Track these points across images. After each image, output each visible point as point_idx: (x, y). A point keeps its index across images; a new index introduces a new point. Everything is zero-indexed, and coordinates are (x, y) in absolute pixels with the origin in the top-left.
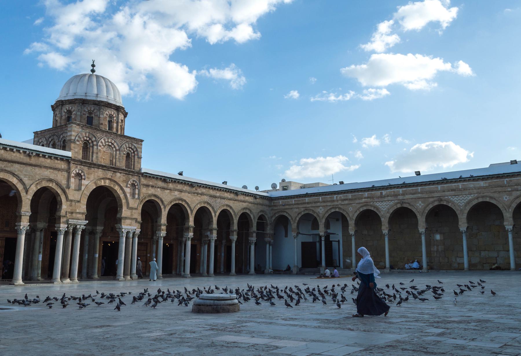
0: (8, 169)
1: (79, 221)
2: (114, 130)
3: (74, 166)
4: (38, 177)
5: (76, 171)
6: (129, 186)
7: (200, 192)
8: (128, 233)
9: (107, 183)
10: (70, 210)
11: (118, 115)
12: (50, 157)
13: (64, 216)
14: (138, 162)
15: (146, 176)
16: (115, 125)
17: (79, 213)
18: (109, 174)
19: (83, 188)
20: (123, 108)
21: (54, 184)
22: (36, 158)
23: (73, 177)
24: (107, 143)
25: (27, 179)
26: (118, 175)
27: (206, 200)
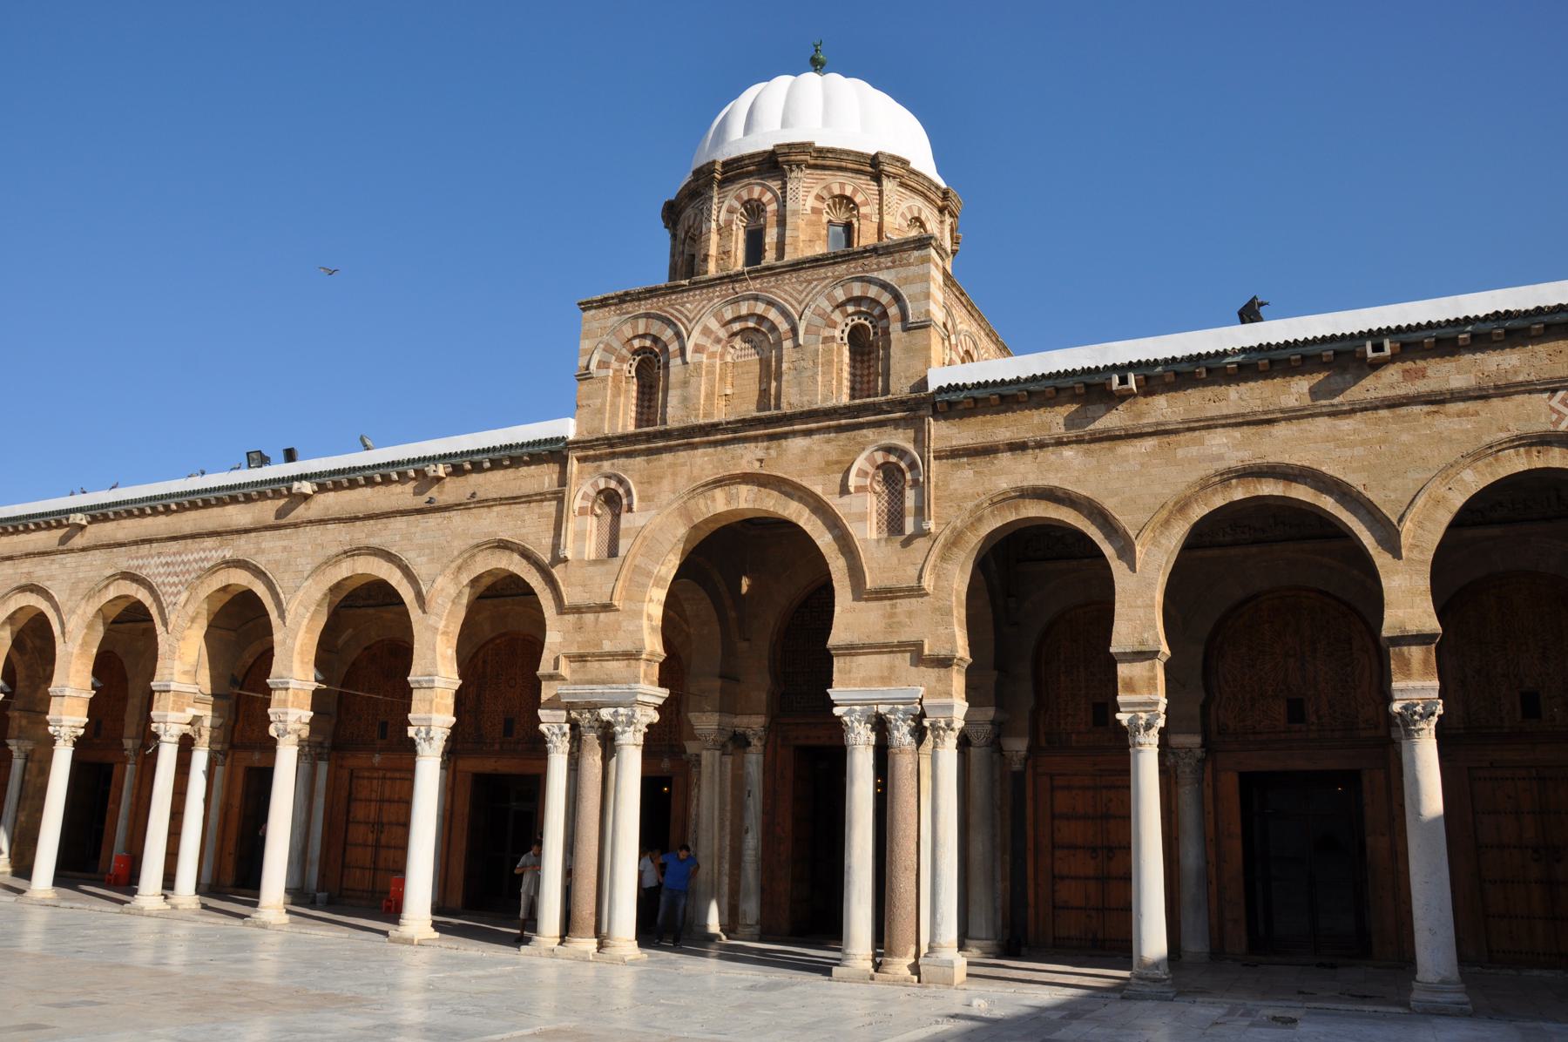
0: (375, 542)
1: (599, 689)
2: (770, 257)
3: (590, 466)
4: (458, 545)
5: (595, 484)
6: (853, 481)
7: (1458, 382)
8: (881, 726)
9: (746, 500)
10: (574, 650)
11: (784, 188)
12: (496, 465)
13: (551, 677)
14: (908, 350)
15: (950, 404)
16: (771, 237)
17: (614, 656)
18: (747, 457)
19: (624, 545)
20: (804, 147)
21: (516, 557)
22: (460, 481)
23: (583, 512)
24: (737, 327)
25: (424, 559)
26: (797, 445)
27: (1542, 425)
